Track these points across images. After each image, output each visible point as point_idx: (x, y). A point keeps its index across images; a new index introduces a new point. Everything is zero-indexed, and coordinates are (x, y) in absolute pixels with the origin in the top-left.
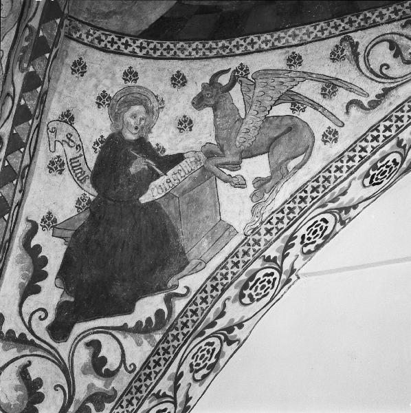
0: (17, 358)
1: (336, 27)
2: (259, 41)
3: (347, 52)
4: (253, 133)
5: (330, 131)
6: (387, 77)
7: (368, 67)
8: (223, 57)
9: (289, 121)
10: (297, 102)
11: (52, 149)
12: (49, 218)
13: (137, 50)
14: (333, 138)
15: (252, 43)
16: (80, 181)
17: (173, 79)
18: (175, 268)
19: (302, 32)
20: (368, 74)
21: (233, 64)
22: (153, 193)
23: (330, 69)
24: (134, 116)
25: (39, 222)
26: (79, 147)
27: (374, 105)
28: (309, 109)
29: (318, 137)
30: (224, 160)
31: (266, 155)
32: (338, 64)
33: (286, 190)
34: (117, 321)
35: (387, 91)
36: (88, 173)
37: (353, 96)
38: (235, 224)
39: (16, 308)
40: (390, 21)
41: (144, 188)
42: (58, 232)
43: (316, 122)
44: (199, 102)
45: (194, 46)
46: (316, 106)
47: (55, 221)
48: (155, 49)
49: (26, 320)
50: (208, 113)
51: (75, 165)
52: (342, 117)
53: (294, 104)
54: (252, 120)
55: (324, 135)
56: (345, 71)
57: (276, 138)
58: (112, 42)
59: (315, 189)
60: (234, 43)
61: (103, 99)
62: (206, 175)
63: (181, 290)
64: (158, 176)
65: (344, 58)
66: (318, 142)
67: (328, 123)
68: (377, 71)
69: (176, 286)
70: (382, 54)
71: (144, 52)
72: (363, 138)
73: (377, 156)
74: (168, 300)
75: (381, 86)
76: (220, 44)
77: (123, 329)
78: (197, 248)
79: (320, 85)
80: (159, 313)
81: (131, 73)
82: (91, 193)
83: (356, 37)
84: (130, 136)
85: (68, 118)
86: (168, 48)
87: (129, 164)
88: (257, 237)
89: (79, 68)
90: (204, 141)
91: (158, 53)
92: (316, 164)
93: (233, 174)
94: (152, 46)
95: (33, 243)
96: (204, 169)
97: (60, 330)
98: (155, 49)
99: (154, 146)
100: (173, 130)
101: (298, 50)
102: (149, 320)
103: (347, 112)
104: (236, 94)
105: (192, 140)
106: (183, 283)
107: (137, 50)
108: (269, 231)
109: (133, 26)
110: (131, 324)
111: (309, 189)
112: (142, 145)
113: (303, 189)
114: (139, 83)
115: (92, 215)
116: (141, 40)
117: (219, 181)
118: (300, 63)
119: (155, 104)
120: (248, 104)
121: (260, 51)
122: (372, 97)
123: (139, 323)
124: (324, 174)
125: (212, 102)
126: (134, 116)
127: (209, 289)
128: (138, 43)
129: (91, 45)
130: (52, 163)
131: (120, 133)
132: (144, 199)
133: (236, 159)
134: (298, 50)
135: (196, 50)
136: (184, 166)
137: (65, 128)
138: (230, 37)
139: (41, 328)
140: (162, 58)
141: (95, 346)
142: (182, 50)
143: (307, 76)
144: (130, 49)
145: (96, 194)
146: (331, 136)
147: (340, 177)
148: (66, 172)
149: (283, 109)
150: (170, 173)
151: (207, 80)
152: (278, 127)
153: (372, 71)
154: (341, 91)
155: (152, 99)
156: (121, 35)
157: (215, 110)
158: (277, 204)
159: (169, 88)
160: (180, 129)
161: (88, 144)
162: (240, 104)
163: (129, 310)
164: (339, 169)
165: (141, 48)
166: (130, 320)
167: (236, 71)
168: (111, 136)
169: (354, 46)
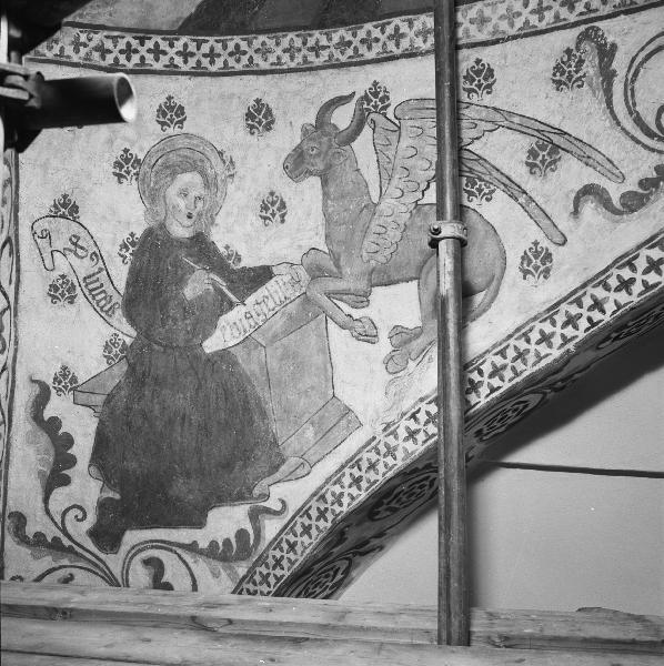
0: (54, 569)
3: (590, 69)
4: (394, 235)
11: (49, 266)
12: (65, 376)
13: (179, 60)
14: (542, 268)
16: (105, 313)
17: (249, 116)
18: (262, 466)
20: (629, 124)
21: (357, 82)
23: (547, 106)
25: (50, 382)
26: (97, 256)
27: (633, 203)
28: (499, 195)
29: (514, 260)
30: (341, 285)
31: (415, 283)
32: (568, 95)
34: (183, 535)
36: (117, 299)
37: (590, 177)
38: (358, 408)
39: (40, 504)
41: (207, 325)
42: (82, 397)
44: (297, 164)
45: (285, 43)
46: (514, 190)
47: (74, 380)
48: (212, 55)
49: (58, 519)
51: (93, 288)
52: (564, 223)
55: (525, 257)
56: (580, 114)
58: (129, 51)
60: (362, 34)
62: (307, 311)
63: (273, 504)
64: (231, 305)
65: (580, 84)
66: (513, 271)
67: (534, 233)
68: (650, 120)
69: (266, 496)
71: (192, 62)
72: (600, 280)
74: (254, 516)
75: (655, 159)
76: (336, 38)
77: (192, 547)
78: (296, 439)
80: (241, 534)
81: (171, 108)
82: (127, 333)
83: (612, 30)
84: (180, 230)
85: (67, 208)
86: (238, 50)
87: (181, 282)
88: (391, 440)
90: (307, 244)
91: (219, 63)
93: (356, 314)
94: (205, 48)
95: (48, 414)
96: (306, 300)
97: (106, 536)
98: (212, 55)
99: (222, 250)
102: (227, 542)
103: (576, 212)
104: (363, 145)
105: (286, 241)
106: (277, 492)
107: (179, 60)
108: (412, 435)
110: (203, 544)
112: (200, 246)
114: (188, 127)
115: (132, 368)
116: (184, 39)
117: (331, 325)
118: (489, 86)
119: (219, 168)
120: (385, 174)
122: (631, 185)
123: (213, 544)
124: (517, 343)
125: (321, 166)
126: (184, 194)
127: (314, 513)
128: (179, 45)
130: (54, 287)
131: (162, 226)
132: (211, 345)
133: (362, 285)
136: (273, 290)
137: (63, 230)
138: (355, 21)
139: (80, 530)
140: (227, 72)
141: (156, 566)
142: (264, 51)
144: (164, 60)
145: (134, 334)
146: (538, 262)
147: (547, 355)
148: (80, 300)
150: (250, 300)
153: (638, 121)
155: (215, 159)
156: (143, 34)
157: (325, 183)
159: (242, 133)
160: (265, 218)
162: (370, 174)
163: (198, 522)
164: (545, 338)
165: (185, 55)
166: (202, 537)
167: (365, 98)
168: (149, 233)
169: (607, 53)
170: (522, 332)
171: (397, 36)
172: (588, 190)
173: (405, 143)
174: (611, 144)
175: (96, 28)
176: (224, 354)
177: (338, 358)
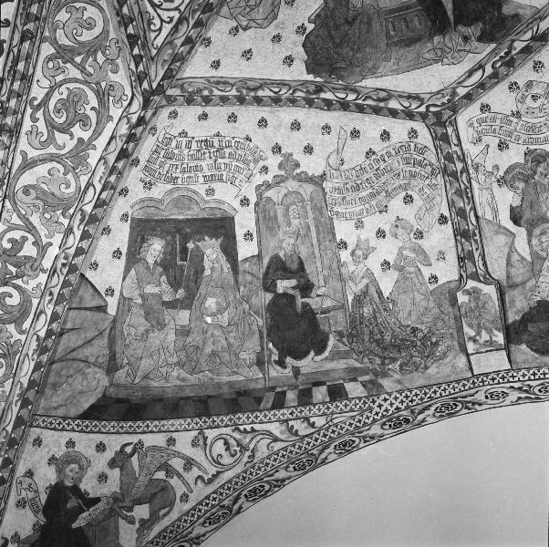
1: (197, 424)
2: (152, 425)
3: (201, 442)
4: (142, 488)
5: (184, 494)
6: (220, 464)
7: (210, 451)
8: (129, 433)
9: (163, 484)
10: (170, 471)
13: (75, 427)
15: (148, 426)
16: (35, 512)
17: (97, 446)
19: (177, 423)
20: (210, 459)
21: (134, 439)
22: (80, 522)
24: (71, 471)
25: (9, 538)
26: (36, 491)
27: (211, 481)
28: (175, 477)
30: (124, 504)
31: (148, 505)
32: (194, 449)
33: (157, 529)
35: (218, 473)
36: (41, 507)
37: (201, 474)
40: (226, 426)
43: (180, 489)
44: (112, 464)
45: (112, 424)
46: (180, 476)
48: (87, 426)
50: (117, 471)
51: (33, 504)
52: (192, 486)
53: (167, 473)
54: (143, 480)
55: (181, 497)
56: (197, 454)
57: (156, 494)
58: (59, 424)
59: (171, 532)
60: (137, 424)
61: (52, 460)
64: (84, 511)
66: (178, 500)
67: (185, 489)
68: (215, 458)
70: (219, 447)
71: (80, 428)
73: (208, 515)
76: (129, 424)
79: (183, 462)
82: (42, 520)
83: (207, 432)
84: (68, 483)
85: (30, 474)
86: (96, 426)
87: (66, 502)
89: (38, 442)
90: (113, 490)
91: (89, 429)
92: (174, 515)
93: (128, 514)
94: (85, 424)
98: (87, 426)
100: (95, 481)
101: (175, 435)
103: (196, 483)
104: (135, 459)
107: (75, 427)
109: (73, 412)
111: (168, 531)
112: (75, 489)
113: (165, 530)
114: (76, 449)
115: (42, 534)
116: (78, 421)
121: (152, 432)
122: (210, 476)
126: (71, 471)
128: (76, 423)
129: (46, 428)
130: (19, 502)
131: (62, 482)
132: (74, 526)
133: (131, 505)
134: (175, 435)
135: (113, 427)
137: (28, 480)
138: (135, 420)
140: (91, 432)
142: (104, 426)
143: (178, 454)
144: (71, 427)
146: (185, 498)
148: (27, 507)
149: (161, 475)
150: (92, 509)
151: (118, 449)
152: (157, 487)
153: (213, 458)
154: (195, 469)
155: (84, 460)
156: (65, 418)
157: (121, 470)
158: (151, 537)
159: (94, 452)
161: (42, 489)
162: (136, 468)
165: (78, 425)
167: (136, 444)
168: (57, 484)
170: (179, 519)
171: (148, 426)
172: (200, 477)
173: (148, 459)
174: (206, 464)
175: (50, 416)
176: (80, 529)
177: (121, 531)
